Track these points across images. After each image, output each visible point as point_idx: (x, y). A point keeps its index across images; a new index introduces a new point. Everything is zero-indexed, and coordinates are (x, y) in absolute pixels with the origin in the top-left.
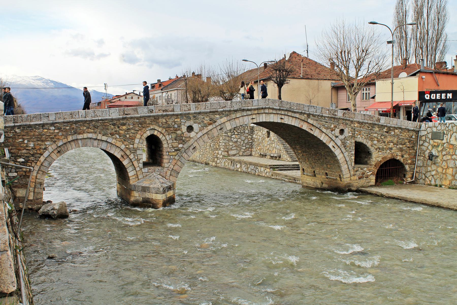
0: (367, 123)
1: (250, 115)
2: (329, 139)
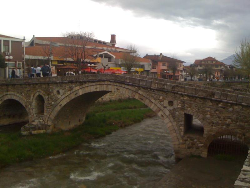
1: (95, 85)
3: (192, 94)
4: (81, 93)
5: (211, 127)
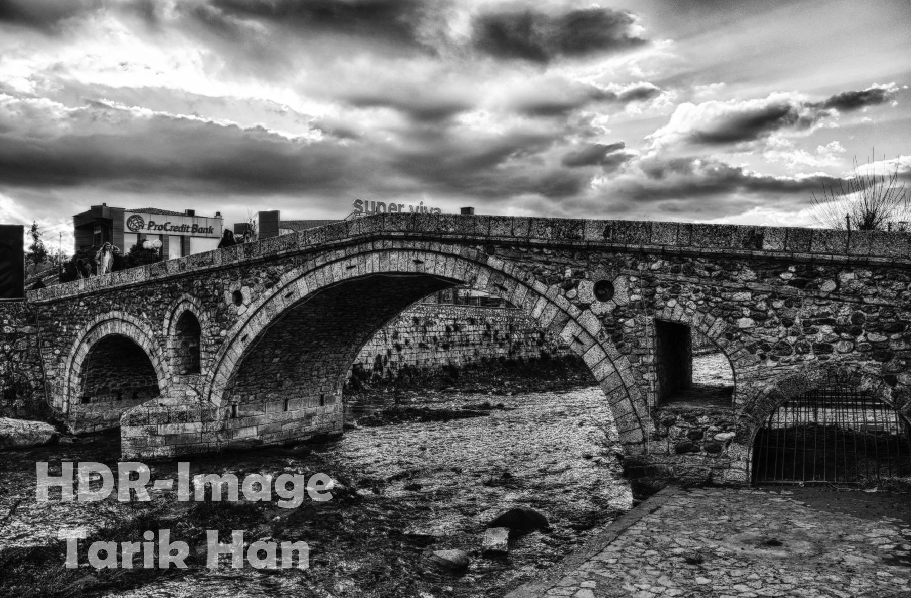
0: (702, 255)
1: (344, 259)
2: (560, 314)
3: (678, 245)
4: (303, 288)
5: (758, 362)
